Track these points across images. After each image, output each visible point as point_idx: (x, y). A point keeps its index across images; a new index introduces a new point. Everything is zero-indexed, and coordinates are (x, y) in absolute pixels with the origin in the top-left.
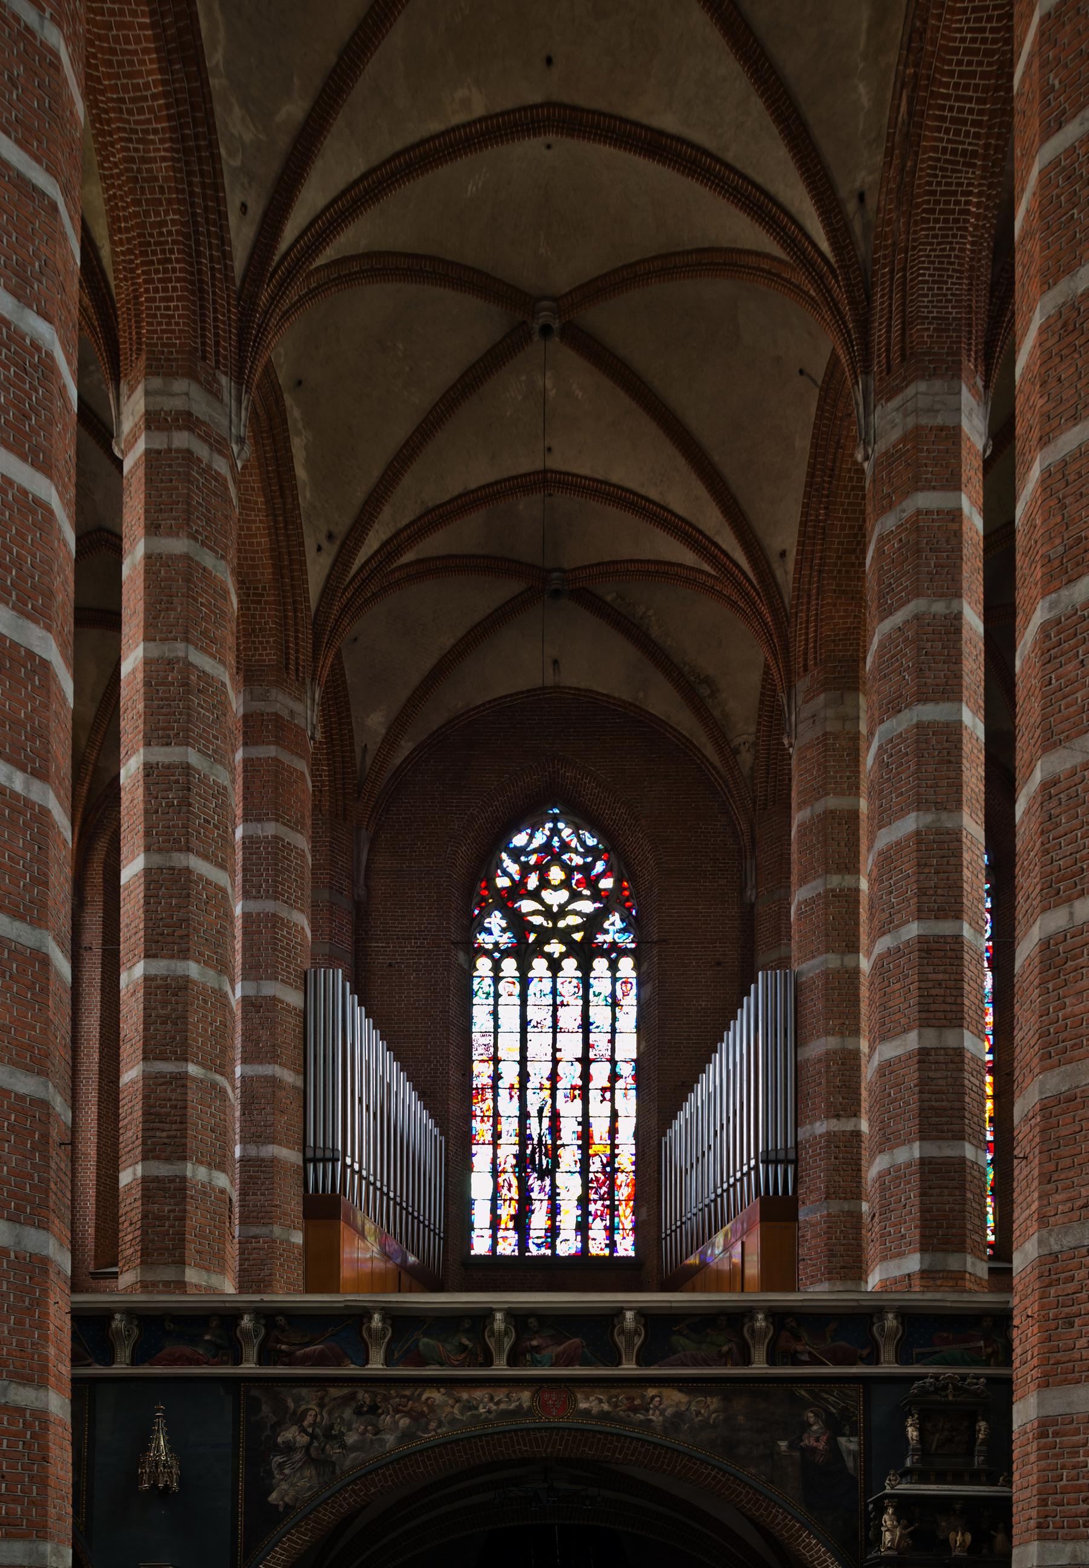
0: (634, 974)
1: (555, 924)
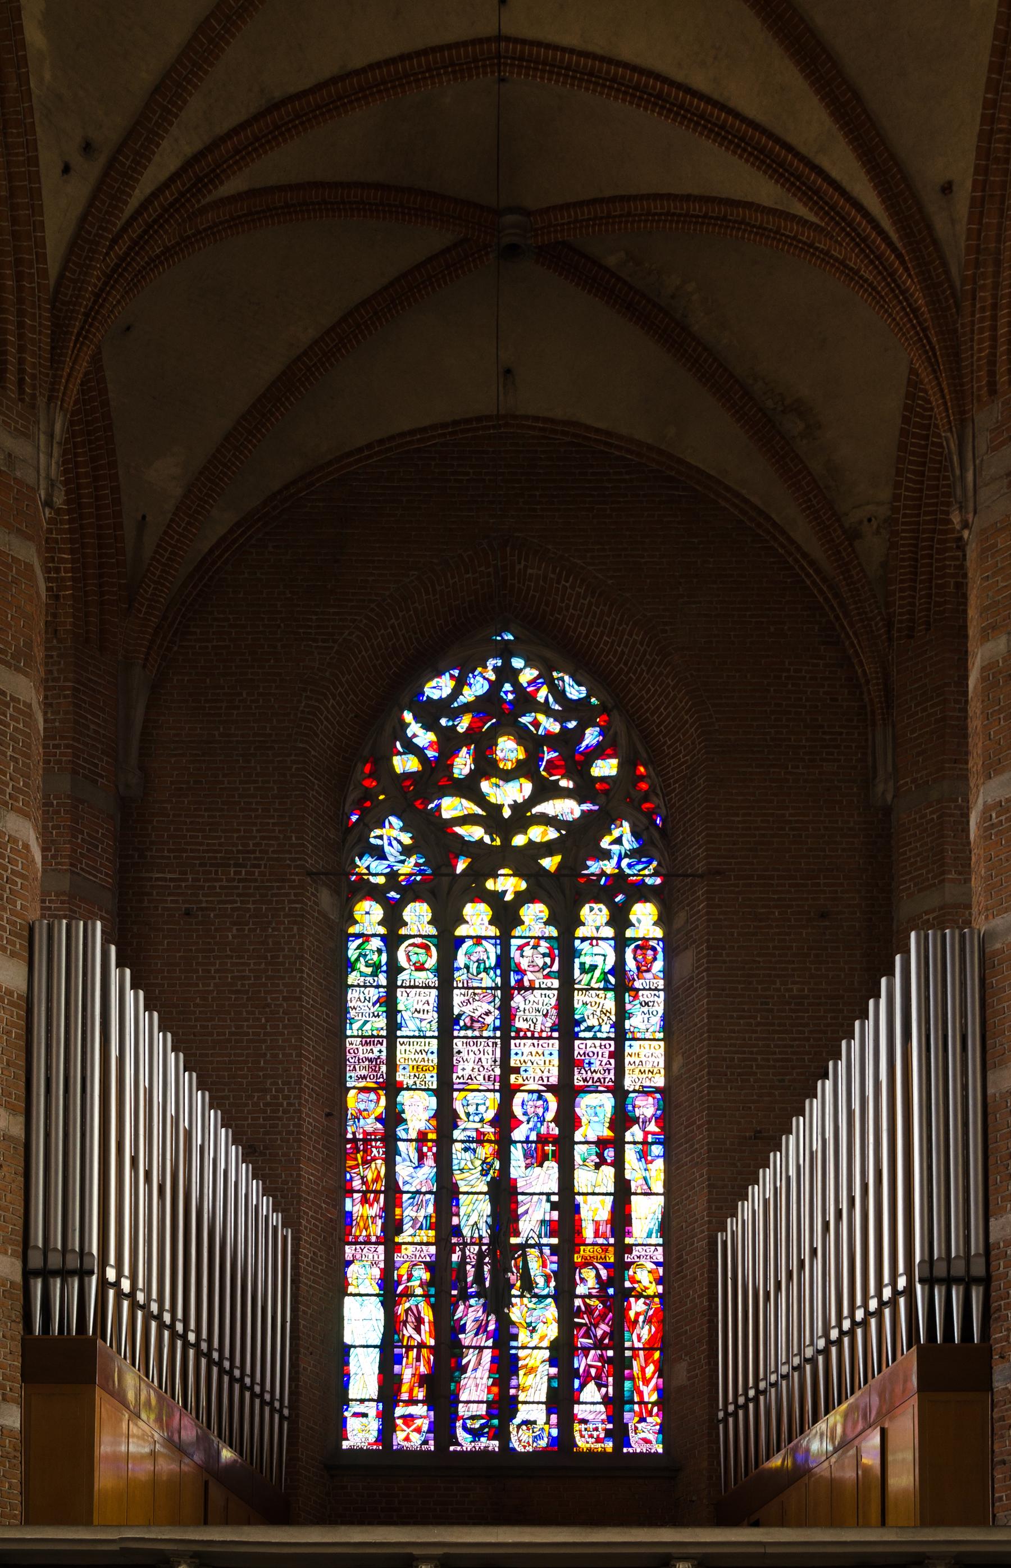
0: (659, 933)
1: (507, 840)
